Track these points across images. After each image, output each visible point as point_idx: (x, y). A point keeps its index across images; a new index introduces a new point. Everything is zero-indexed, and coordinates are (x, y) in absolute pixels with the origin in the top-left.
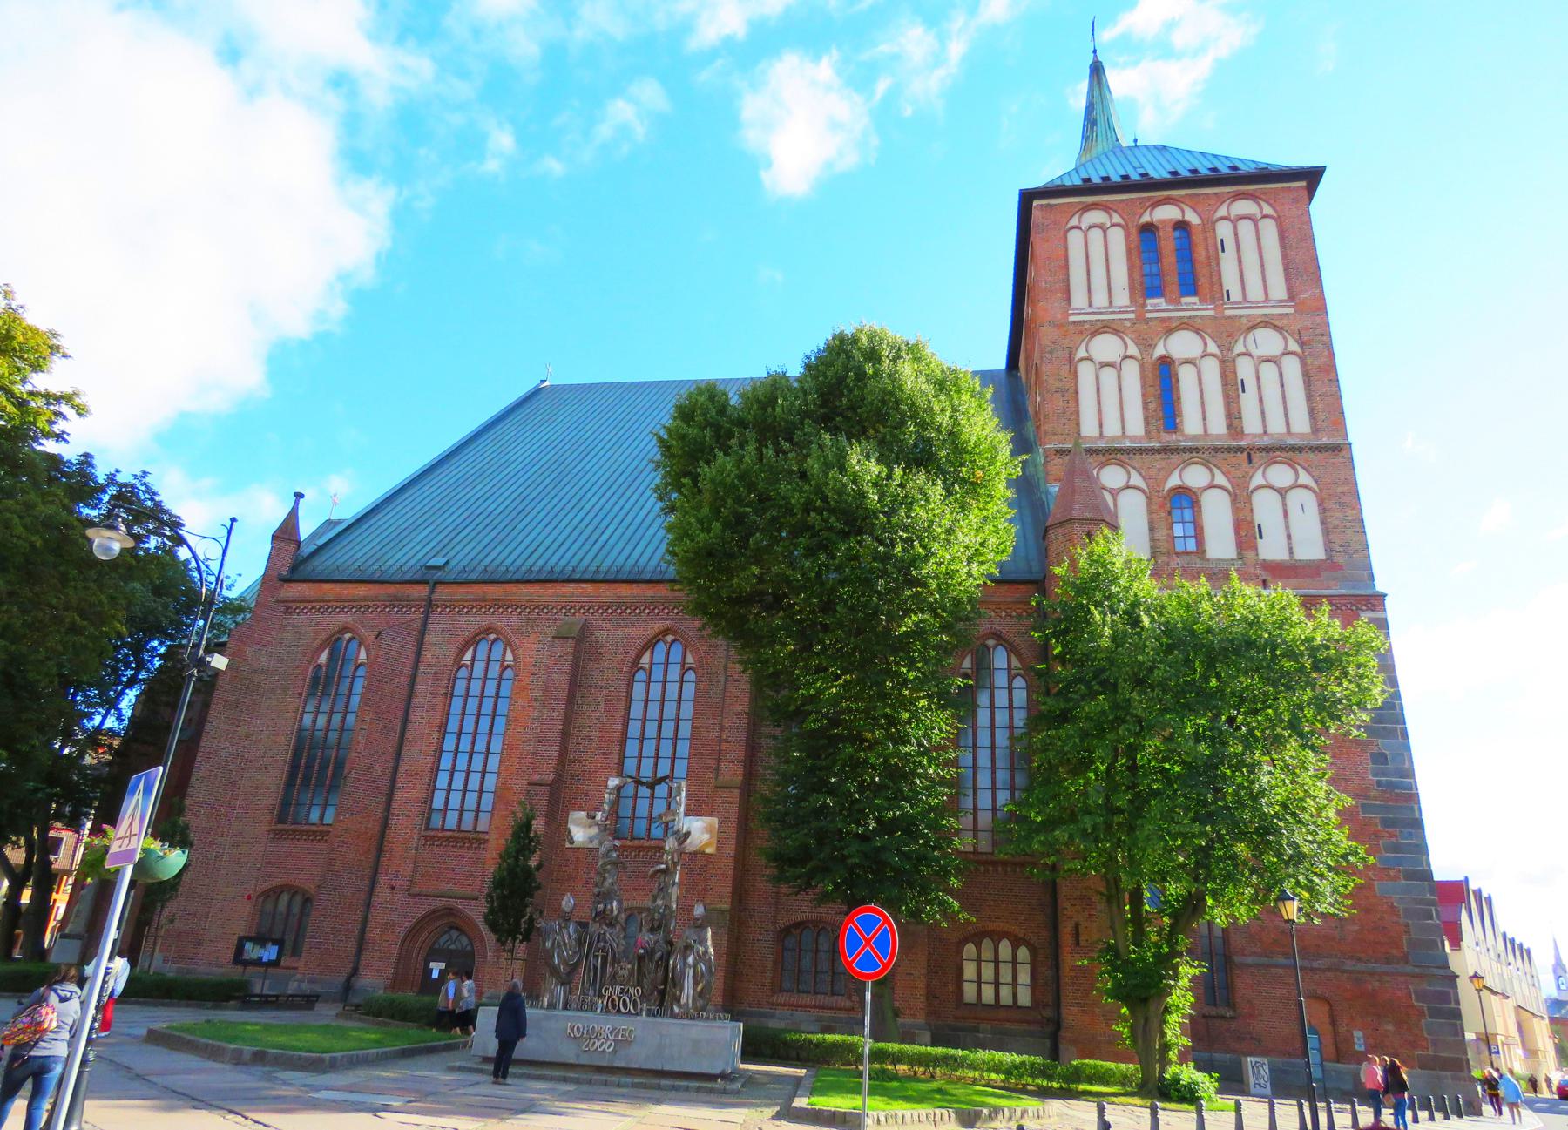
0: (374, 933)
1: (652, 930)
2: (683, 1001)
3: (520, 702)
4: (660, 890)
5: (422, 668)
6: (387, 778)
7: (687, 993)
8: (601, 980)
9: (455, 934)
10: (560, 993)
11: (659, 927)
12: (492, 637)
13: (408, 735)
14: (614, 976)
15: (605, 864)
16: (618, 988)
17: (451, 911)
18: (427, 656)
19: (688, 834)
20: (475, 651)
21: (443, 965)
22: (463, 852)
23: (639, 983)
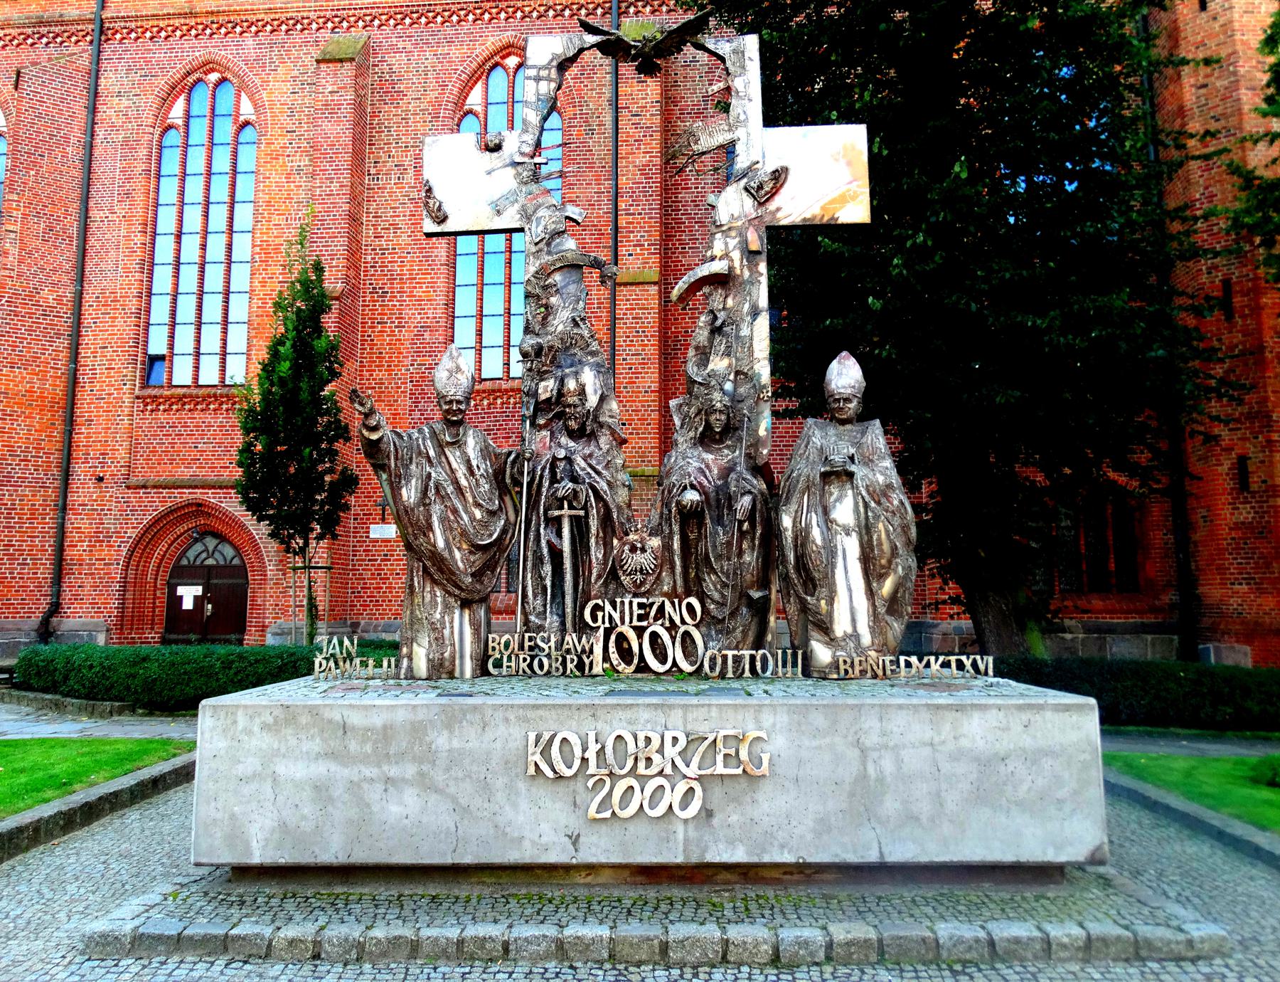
0: (77, 550)
1: (707, 439)
2: (841, 626)
3: (275, 178)
4: (716, 331)
5: (100, 132)
6: (66, 312)
7: (850, 604)
8: (580, 583)
9: (211, 543)
10: (461, 628)
11: (730, 429)
12: (214, 77)
13: (92, 241)
14: (612, 575)
15: (543, 273)
16: (630, 603)
17: (199, 508)
18: (107, 112)
19: (779, 176)
20: (188, 100)
21: (198, 590)
22: (209, 418)
23: (693, 586)
